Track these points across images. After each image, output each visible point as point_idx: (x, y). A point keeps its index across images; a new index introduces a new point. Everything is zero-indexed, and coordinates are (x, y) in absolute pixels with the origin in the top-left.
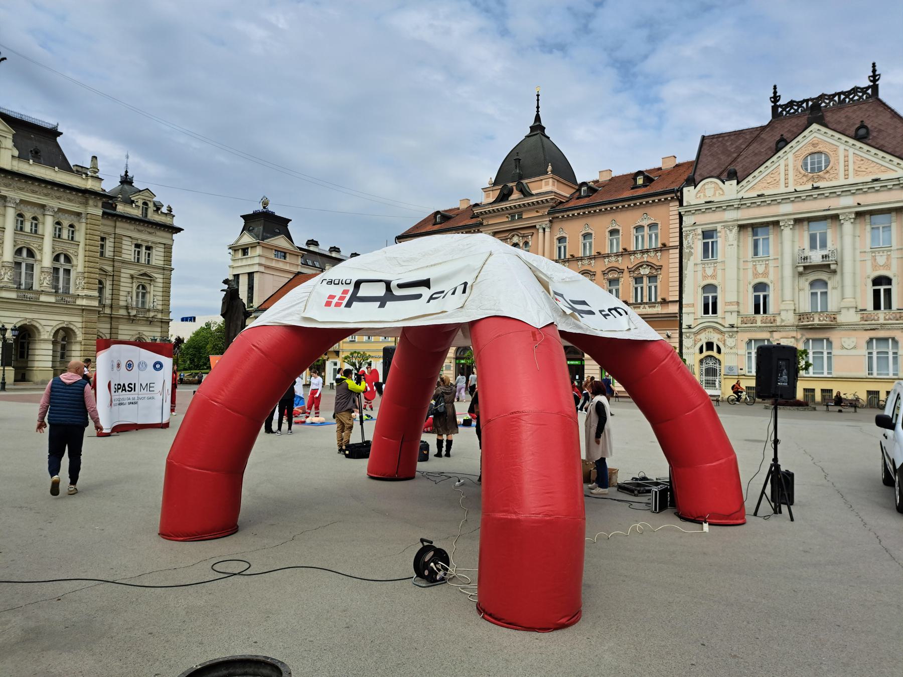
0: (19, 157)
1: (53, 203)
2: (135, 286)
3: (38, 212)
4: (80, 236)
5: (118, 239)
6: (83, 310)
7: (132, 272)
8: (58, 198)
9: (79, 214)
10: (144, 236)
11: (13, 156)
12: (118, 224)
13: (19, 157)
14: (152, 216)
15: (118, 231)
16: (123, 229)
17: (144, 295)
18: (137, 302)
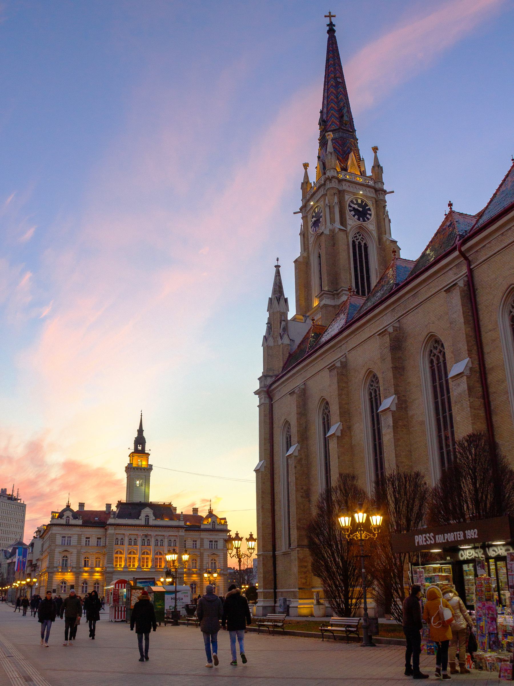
0: (155, 519)
1: (166, 534)
2: (210, 559)
3: (162, 537)
4: (178, 544)
5: (202, 540)
7: (207, 553)
8: (168, 531)
9: (177, 536)
10: (214, 536)
12: (202, 534)
13: (155, 519)
14: (218, 527)
15: (202, 537)
16: (204, 535)
17: (215, 563)
18: (212, 566)
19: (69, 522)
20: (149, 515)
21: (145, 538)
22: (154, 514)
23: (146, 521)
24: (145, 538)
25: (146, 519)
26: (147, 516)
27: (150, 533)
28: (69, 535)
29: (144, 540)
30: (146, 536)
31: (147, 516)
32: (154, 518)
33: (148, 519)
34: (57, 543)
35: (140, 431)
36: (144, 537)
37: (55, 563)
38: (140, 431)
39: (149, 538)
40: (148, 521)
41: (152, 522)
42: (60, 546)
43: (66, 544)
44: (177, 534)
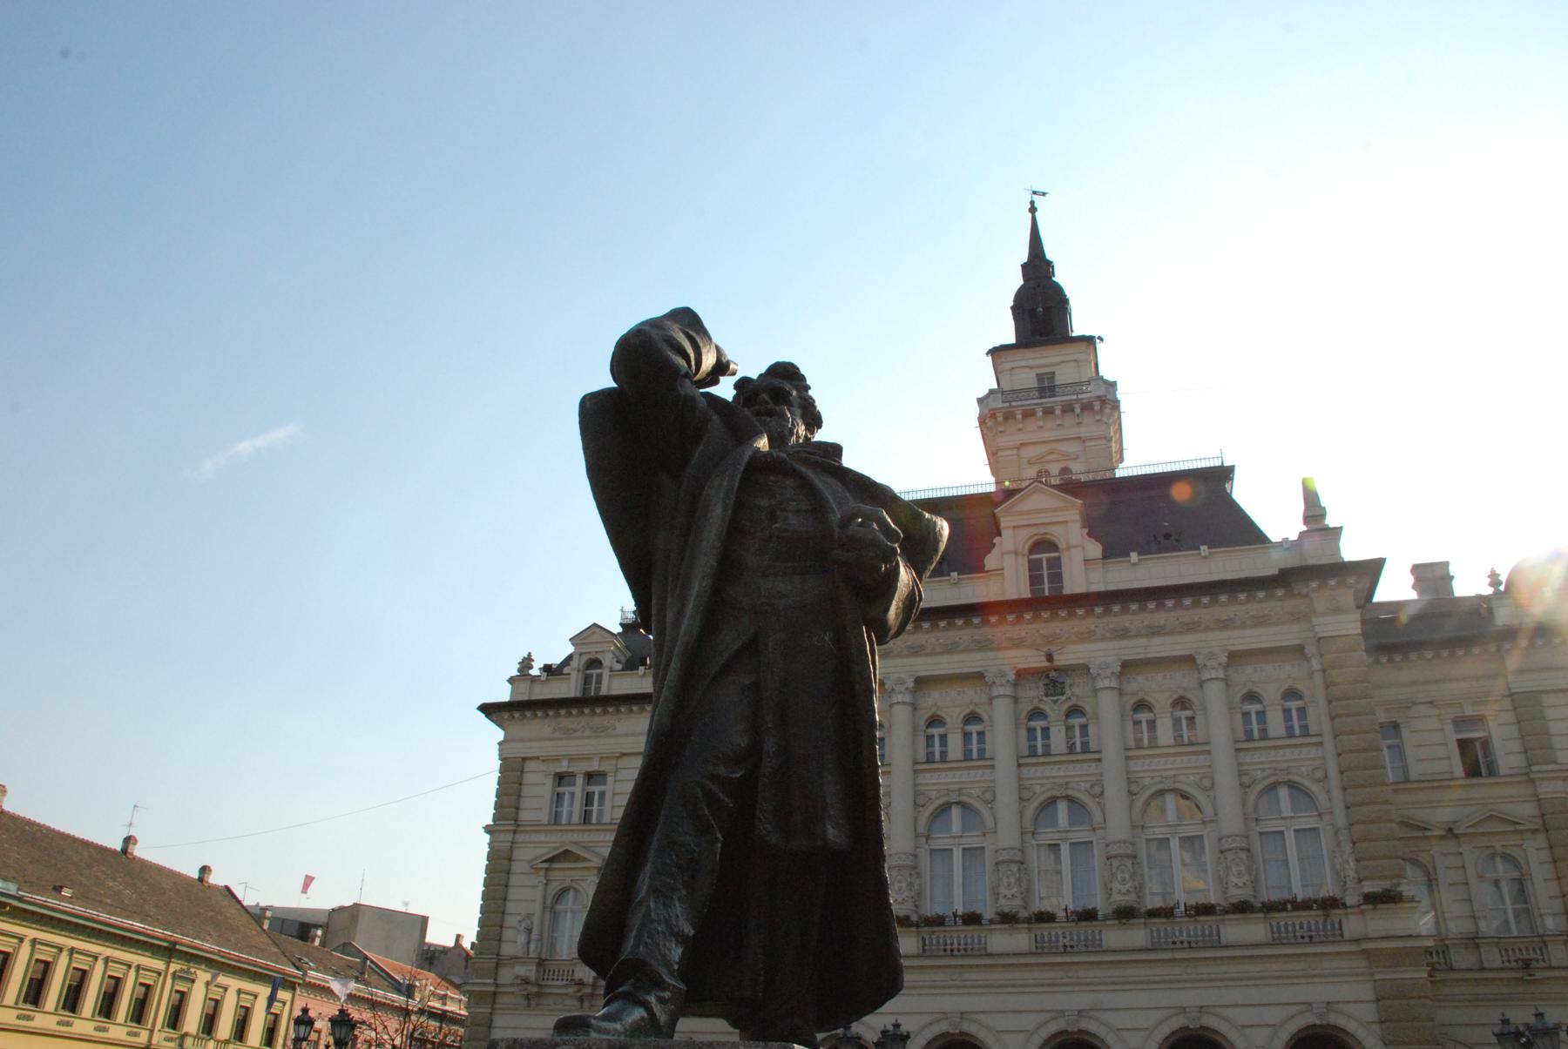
0: (1110, 553)
3: (1178, 680)
6: (1366, 953)
9: (1298, 651)
11: (1087, 561)
19: (598, 689)
20: (1056, 534)
21: (1047, 705)
22: (1094, 528)
23: (1035, 580)
24: (1047, 705)
25: (1034, 566)
26: (1043, 545)
27: (1069, 655)
28: (594, 766)
29: (1036, 714)
30: (1053, 679)
31: (1043, 545)
32: (1095, 549)
33: (1055, 564)
34: (524, 816)
35: (1037, 268)
36: (1033, 694)
37: (508, 934)
38: (1037, 268)
39: (1077, 691)
40: (1057, 578)
41: (1076, 581)
42: (537, 828)
43: (575, 819)
44: (1287, 635)
